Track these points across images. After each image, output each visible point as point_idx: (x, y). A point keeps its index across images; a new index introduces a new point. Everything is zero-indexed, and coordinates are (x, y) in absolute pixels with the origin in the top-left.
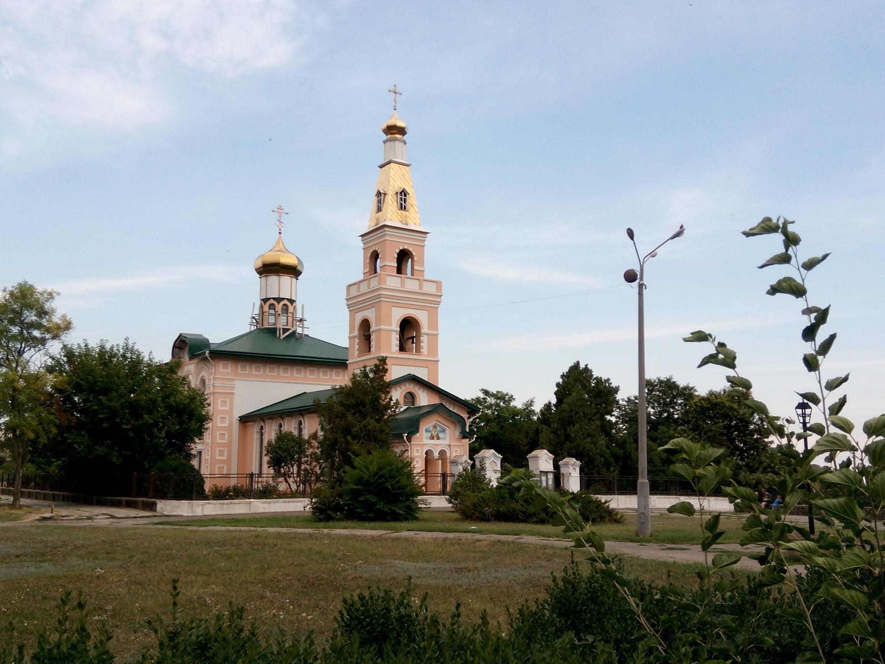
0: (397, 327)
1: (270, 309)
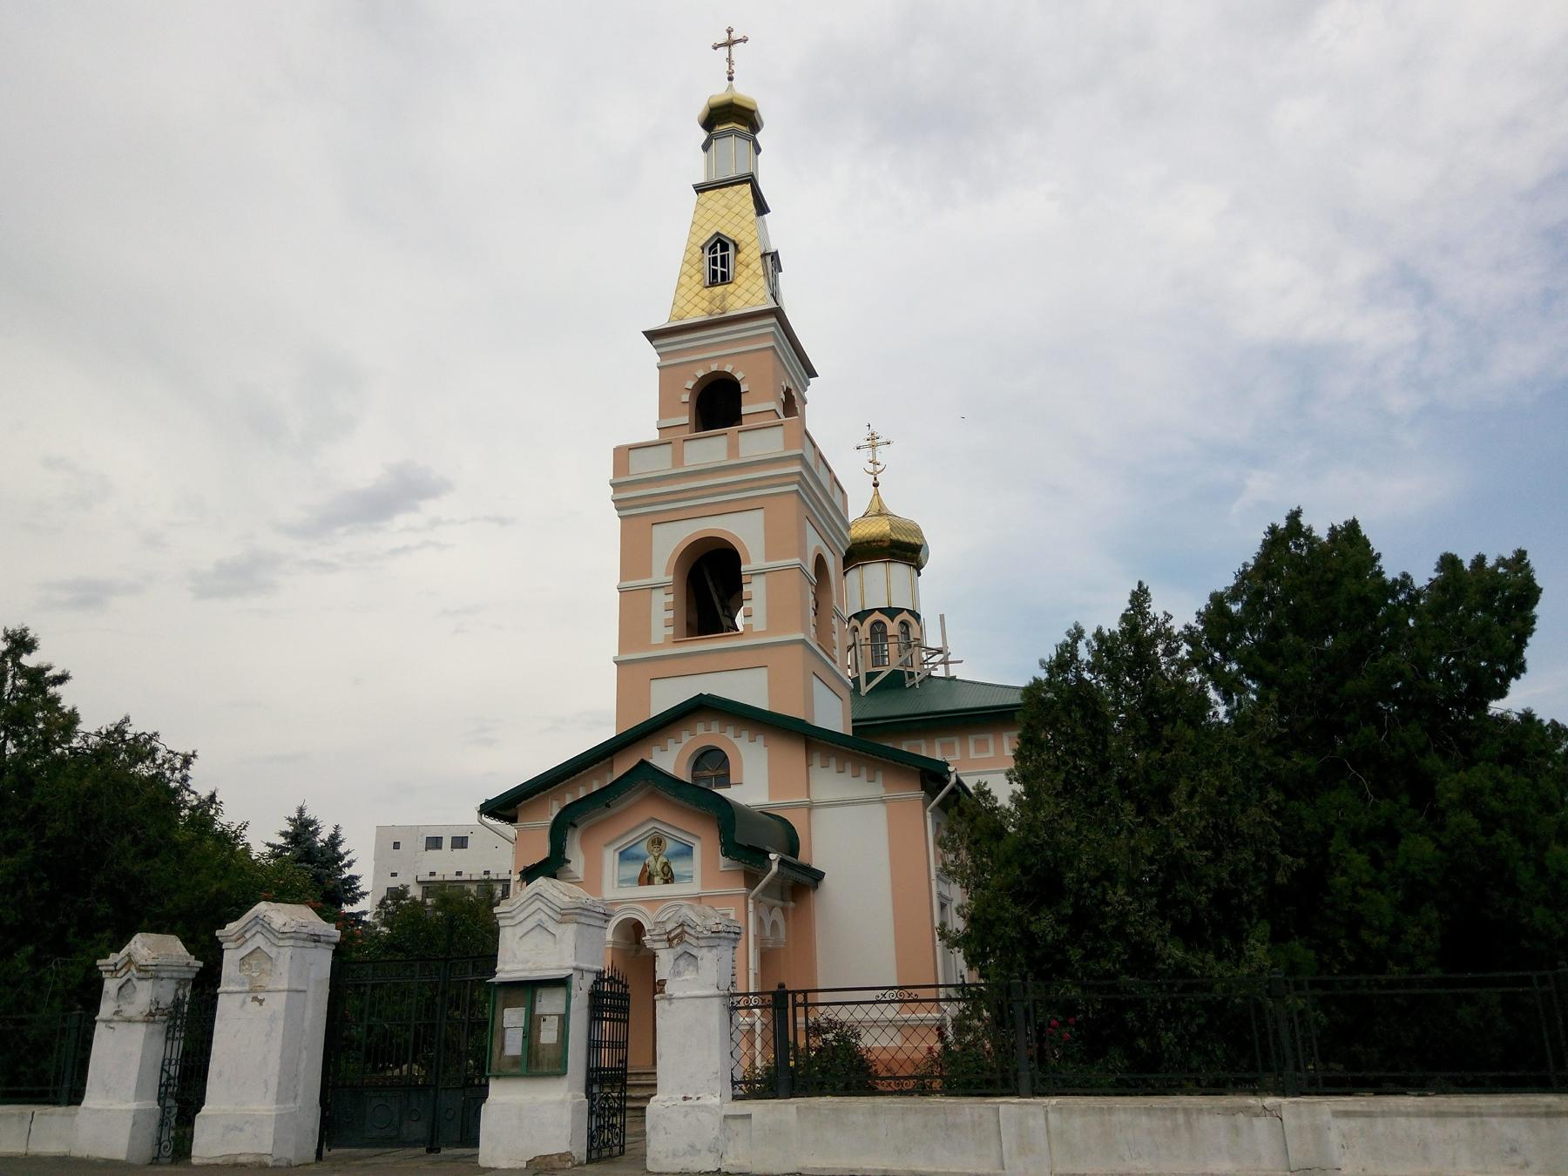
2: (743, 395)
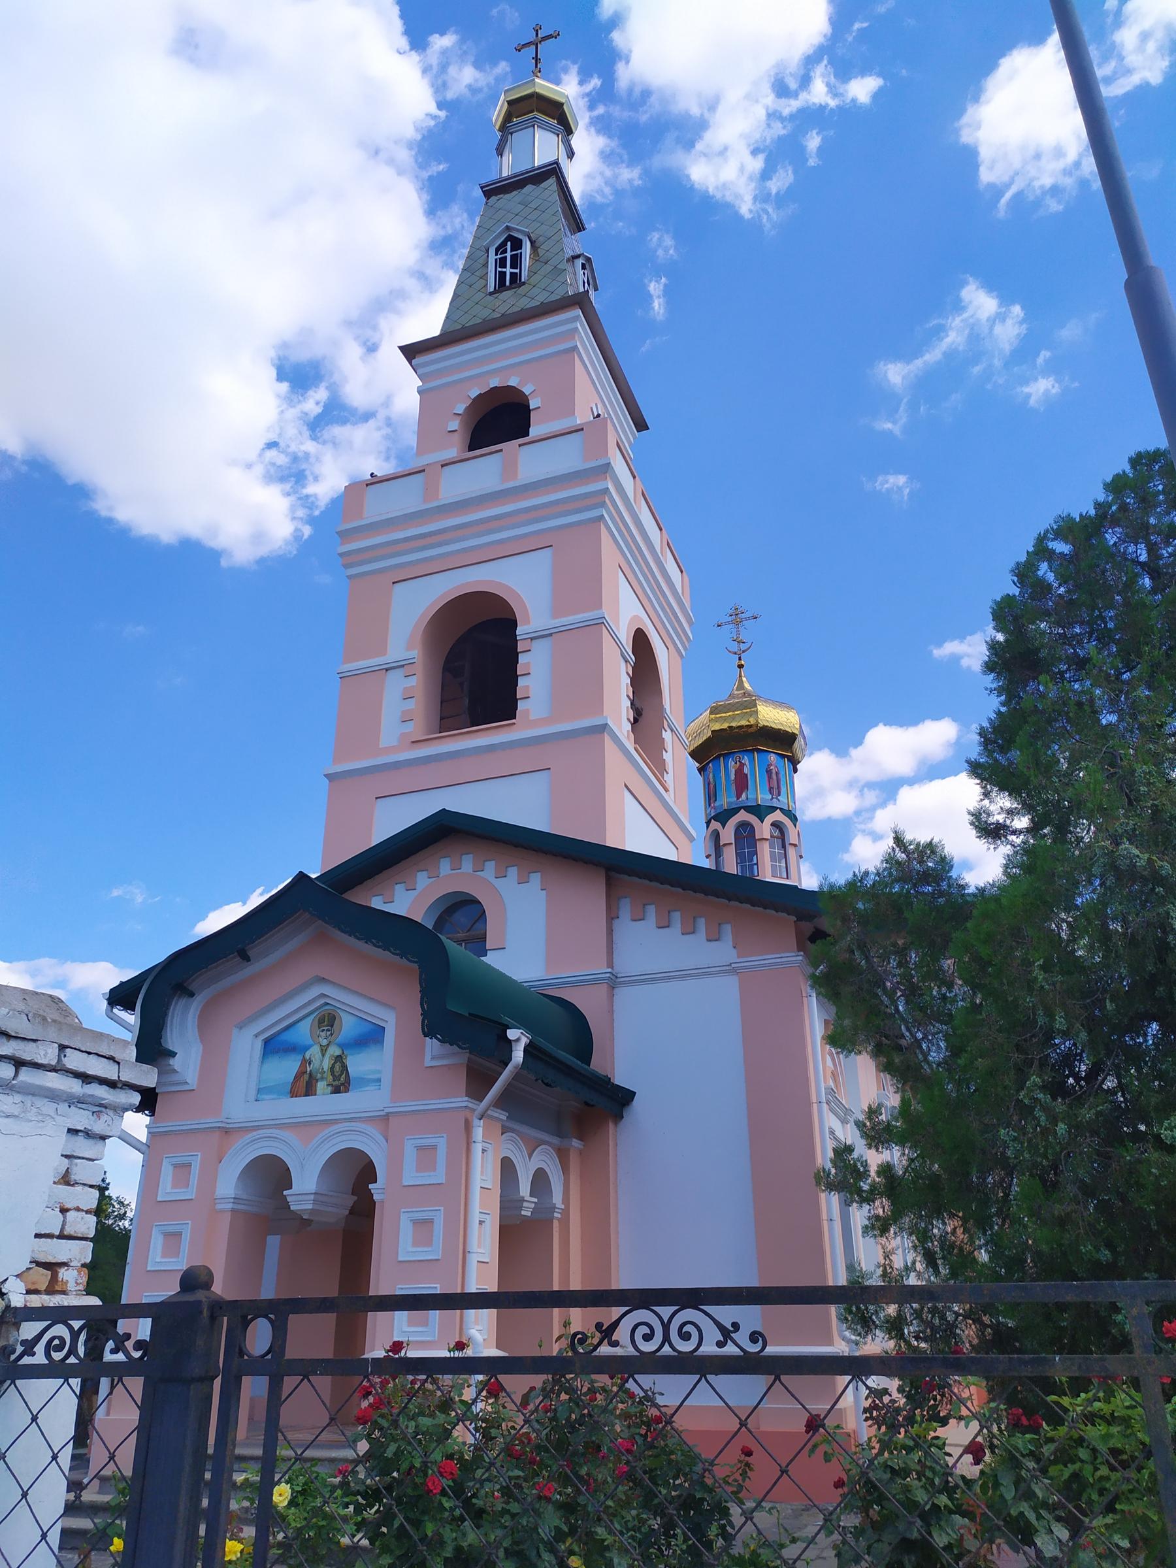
0: (409, 648)
2: (532, 414)
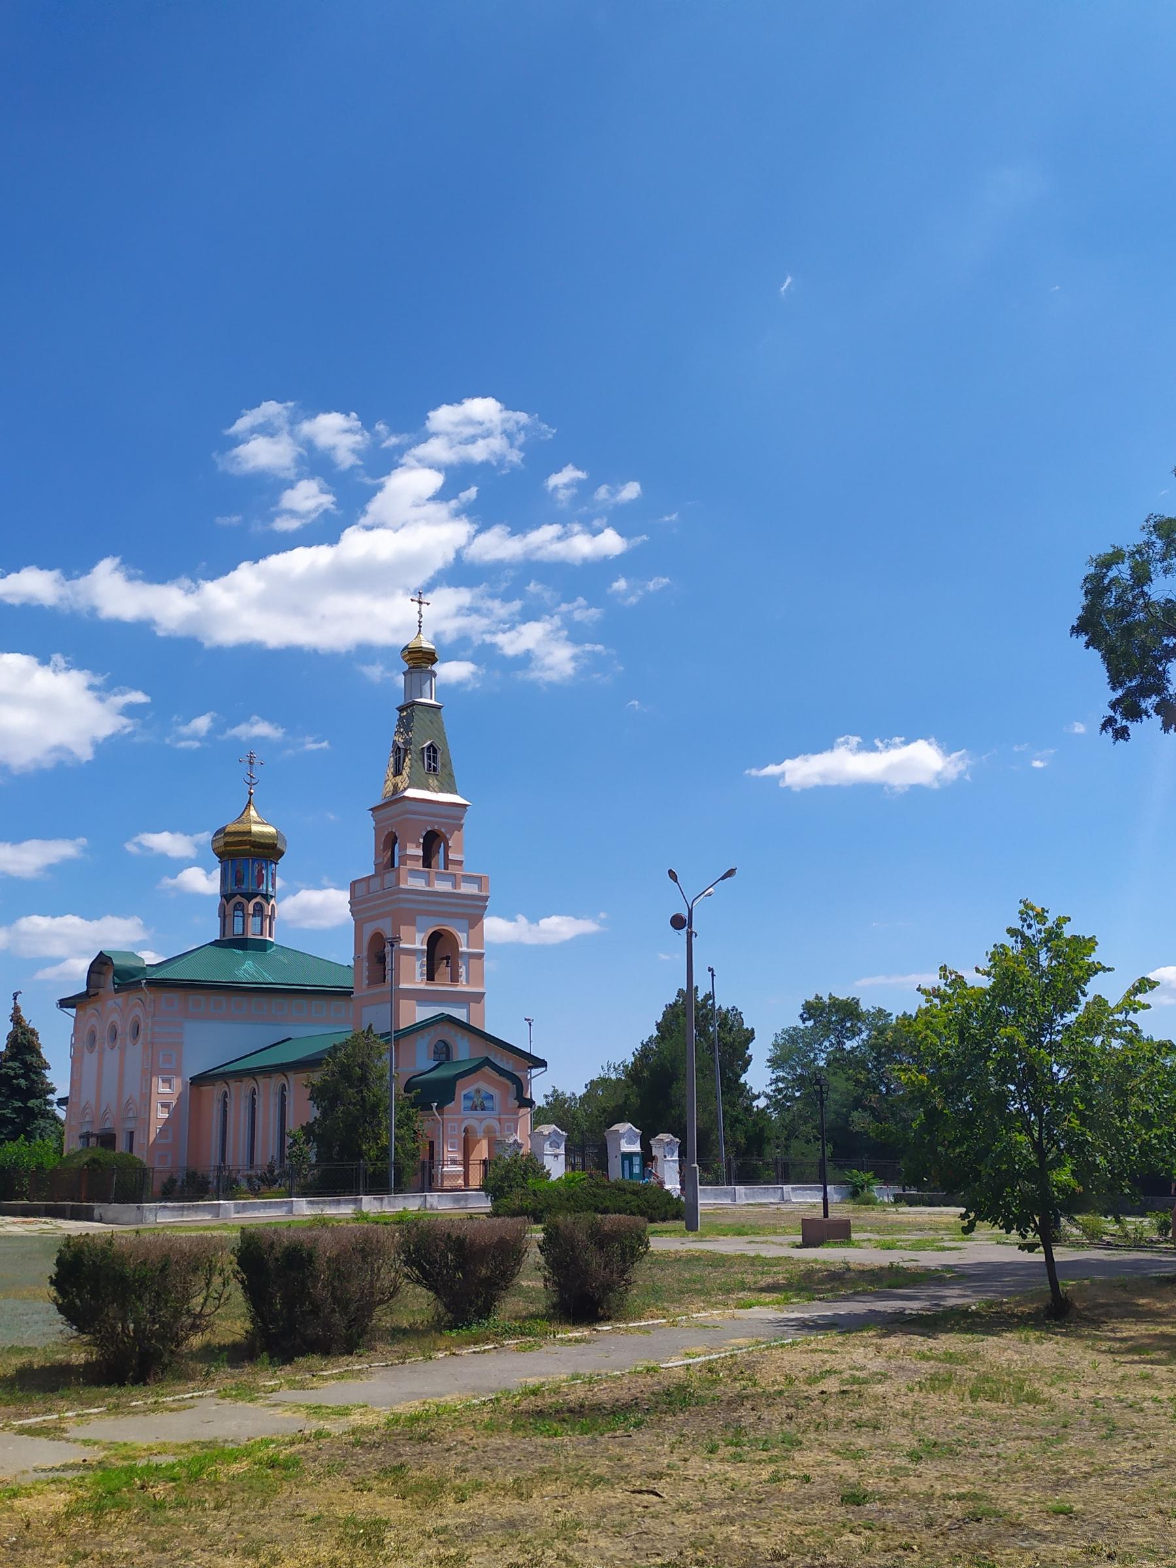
0: (422, 944)
1: (235, 909)
